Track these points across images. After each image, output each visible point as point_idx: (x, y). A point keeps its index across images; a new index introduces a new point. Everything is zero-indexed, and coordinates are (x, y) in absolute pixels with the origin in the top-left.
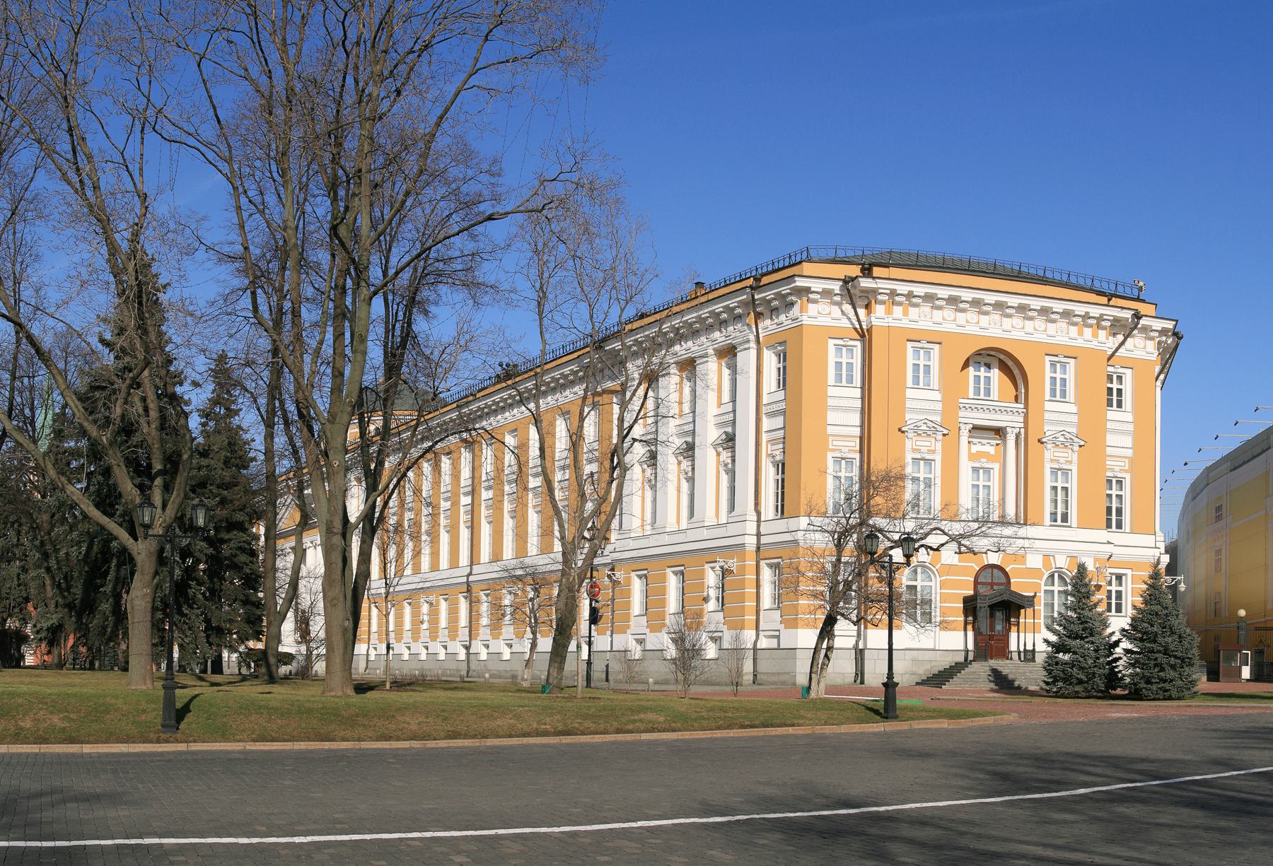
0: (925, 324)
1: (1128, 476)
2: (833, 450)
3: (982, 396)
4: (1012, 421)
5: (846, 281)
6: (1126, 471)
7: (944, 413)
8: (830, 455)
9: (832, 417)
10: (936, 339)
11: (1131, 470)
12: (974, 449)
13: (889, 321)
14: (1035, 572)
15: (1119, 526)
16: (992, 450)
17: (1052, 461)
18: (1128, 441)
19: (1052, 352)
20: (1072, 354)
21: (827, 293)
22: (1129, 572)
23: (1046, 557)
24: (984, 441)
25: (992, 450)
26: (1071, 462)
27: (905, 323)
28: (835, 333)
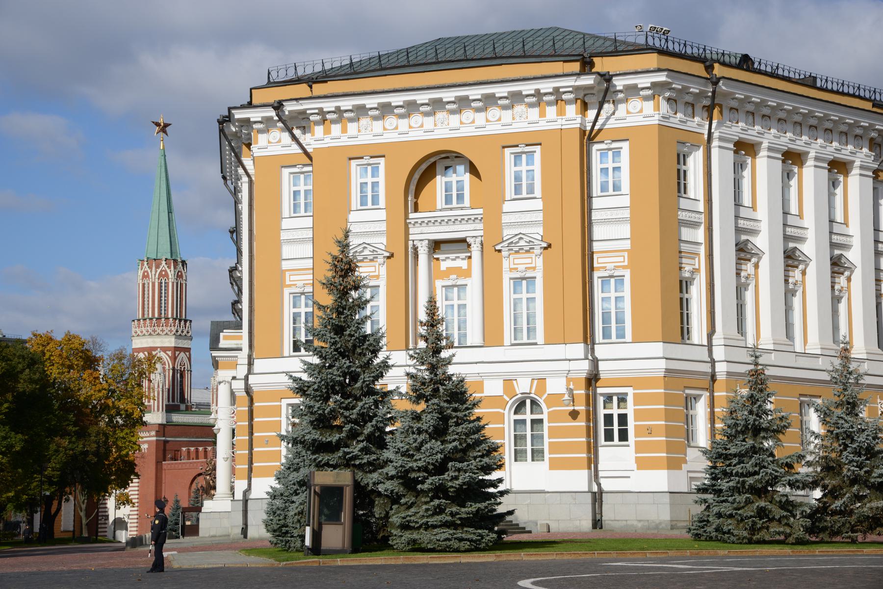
0: (365, 139)
1: (627, 273)
2: (290, 286)
3: (454, 204)
4: (472, 231)
5: (278, 106)
6: (624, 267)
7: (389, 233)
8: (287, 291)
9: (287, 251)
10: (377, 152)
11: (632, 265)
12: (444, 266)
13: (328, 142)
14: (497, 401)
15: (621, 334)
16: (464, 264)
17: (511, 270)
18: (625, 230)
19: (509, 142)
20: (533, 140)
21: (267, 121)
22: (630, 391)
23: (508, 383)
24: (453, 256)
25: (464, 264)
26: (534, 268)
27: (344, 141)
28: (286, 162)
